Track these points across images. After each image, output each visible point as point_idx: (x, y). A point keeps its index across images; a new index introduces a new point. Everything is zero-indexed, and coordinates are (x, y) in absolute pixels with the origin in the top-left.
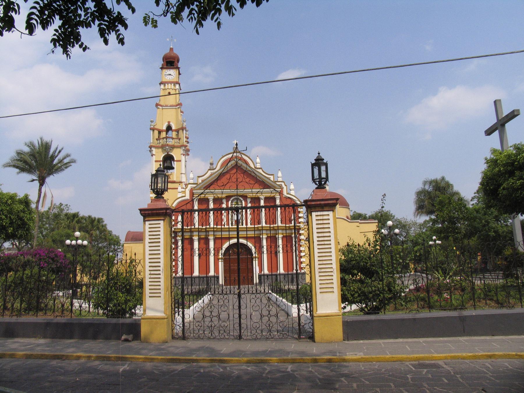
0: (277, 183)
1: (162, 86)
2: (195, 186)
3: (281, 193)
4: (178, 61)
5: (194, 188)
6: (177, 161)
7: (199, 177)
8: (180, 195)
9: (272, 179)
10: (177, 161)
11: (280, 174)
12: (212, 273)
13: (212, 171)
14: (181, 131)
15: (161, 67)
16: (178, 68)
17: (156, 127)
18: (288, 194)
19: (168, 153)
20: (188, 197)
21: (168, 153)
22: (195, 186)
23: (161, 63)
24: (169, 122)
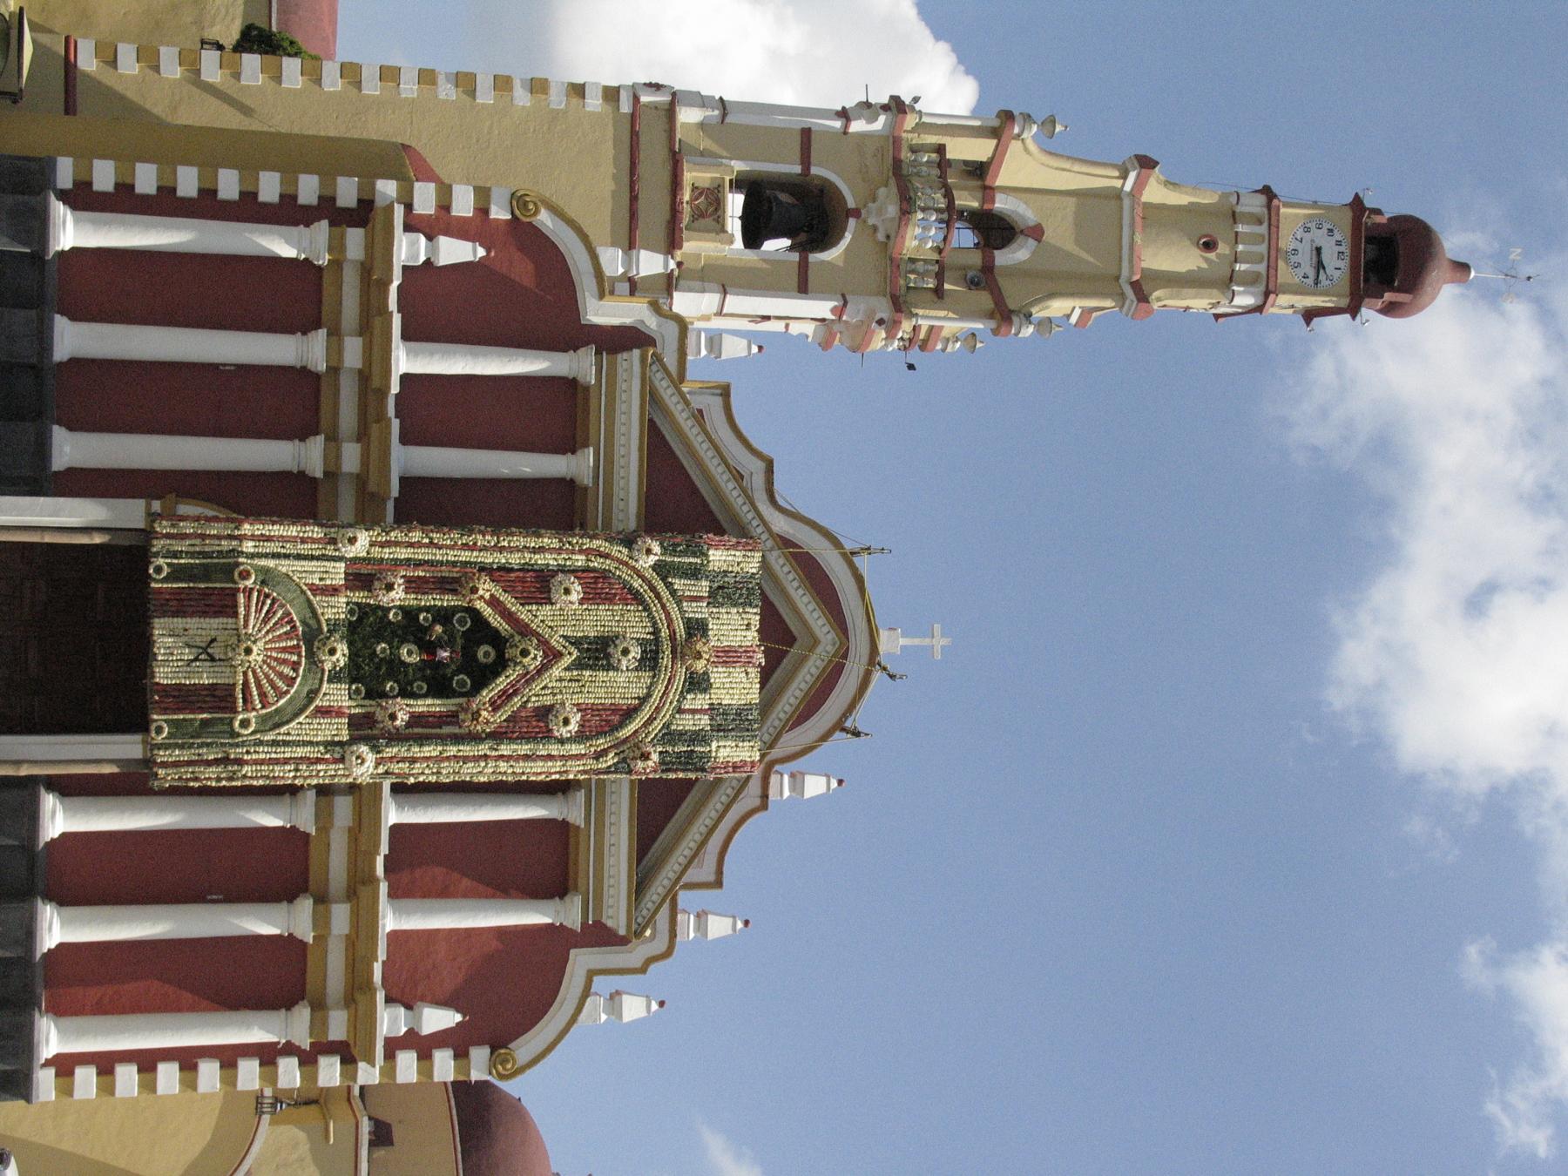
0: (666, 906)
1: (1255, 204)
2: (670, 360)
3: (598, 935)
4: (1390, 310)
5: (658, 358)
6: (803, 266)
7: (725, 392)
8: (613, 261)
9: (692, 875)
10: (803, 266)
11: (719, 927)
12: (70, 449)
13: (758, 481)
14: (984, 299)
15: (1368, 203)
16: (1353, 310)
17: (1015, 146)
18: (591, 974)
19: (856, 213)
20: (601, 313)
21: (856, 213)
22: (670, 360)
23: (1390, 203)
24: (1037, 232)
